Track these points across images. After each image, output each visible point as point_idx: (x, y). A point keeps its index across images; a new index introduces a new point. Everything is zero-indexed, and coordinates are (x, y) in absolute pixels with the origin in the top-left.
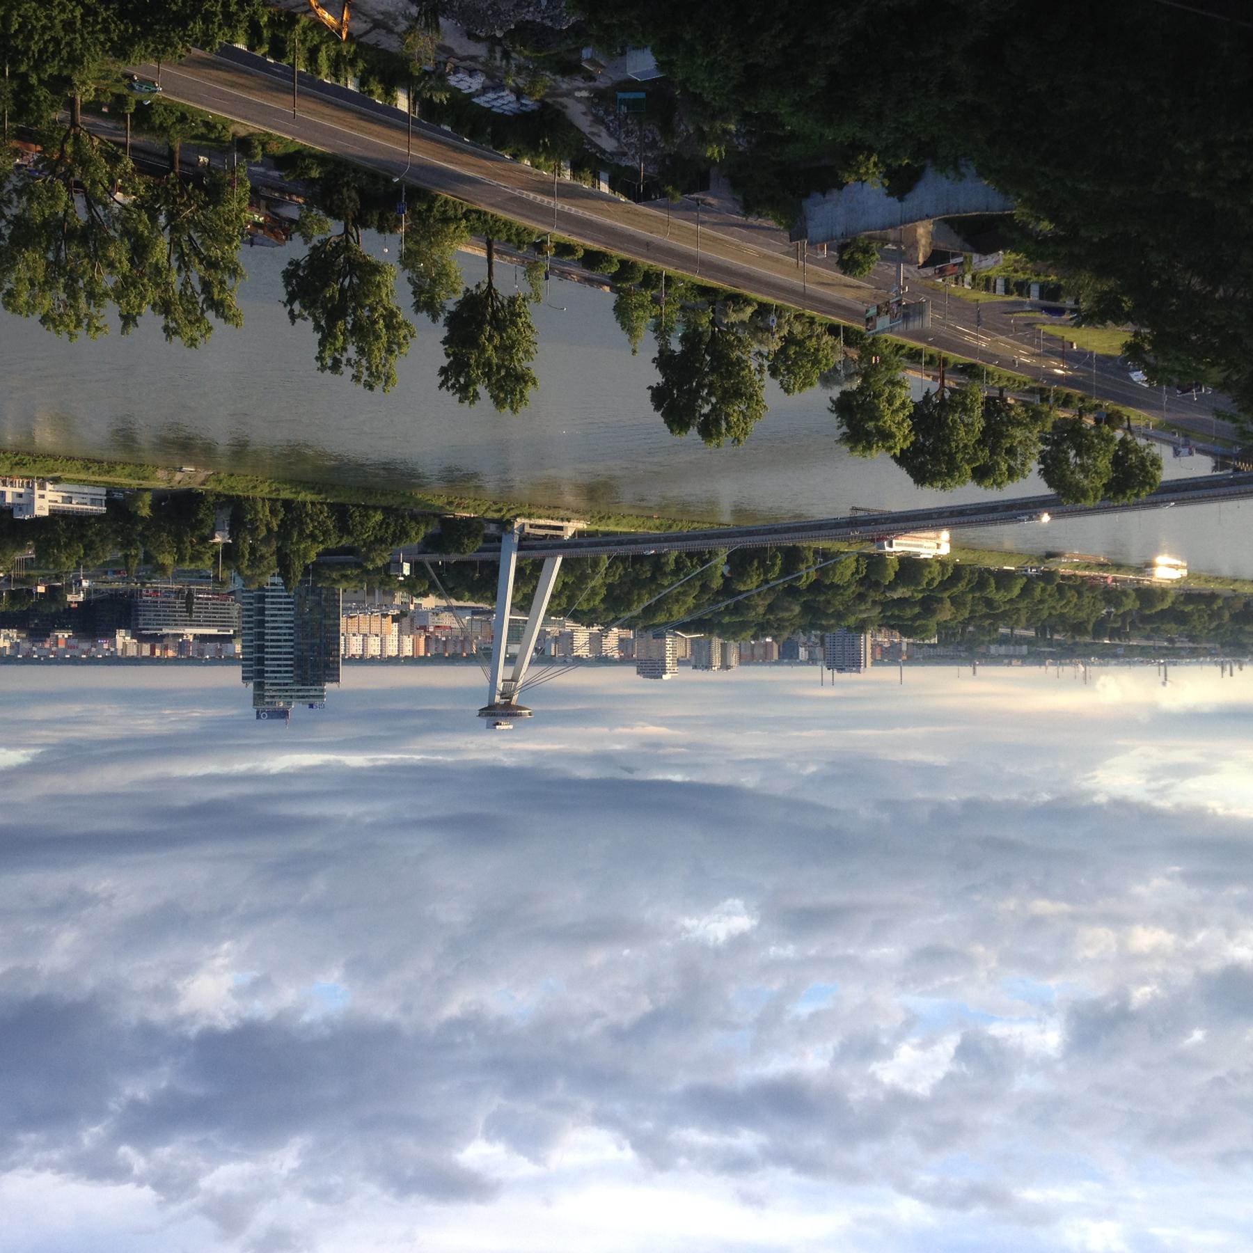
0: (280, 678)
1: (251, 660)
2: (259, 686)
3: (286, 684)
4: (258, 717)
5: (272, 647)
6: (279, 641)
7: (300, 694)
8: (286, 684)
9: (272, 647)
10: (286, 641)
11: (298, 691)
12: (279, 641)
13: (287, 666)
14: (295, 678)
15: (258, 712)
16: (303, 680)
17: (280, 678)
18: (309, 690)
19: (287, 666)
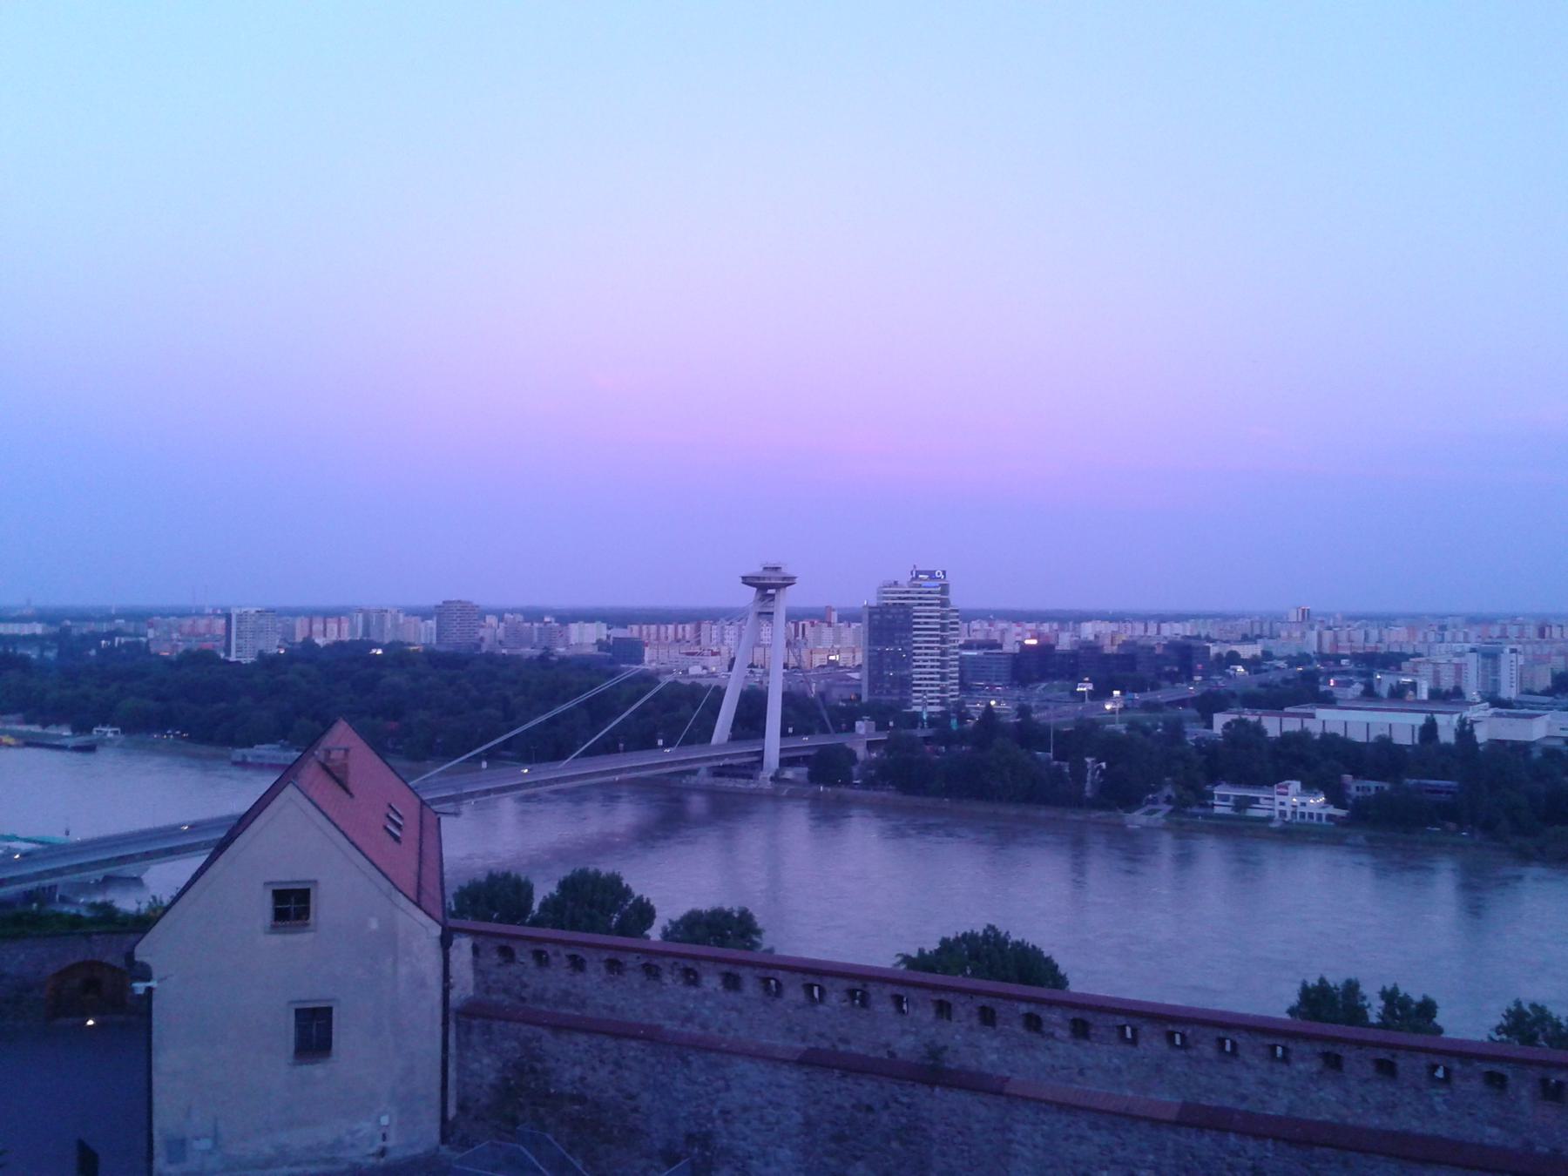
0: (925, 611)
1: (953, 629)
2: (944, 603)
3: (920, 605)
4: (944, 573)
5: (933, 642)
6: (927, 648)
7: (906, 595)
8: (920, 605)
9: (933, 642)
10: (920, 648)
11: (905, 599)
12: (927, 648)
13: (918, 623)
14: (911, 611)
15: (945, 577)
16: (906, 611)
17: (925, 611)
18: (900, 598)
19: (918, 623)
